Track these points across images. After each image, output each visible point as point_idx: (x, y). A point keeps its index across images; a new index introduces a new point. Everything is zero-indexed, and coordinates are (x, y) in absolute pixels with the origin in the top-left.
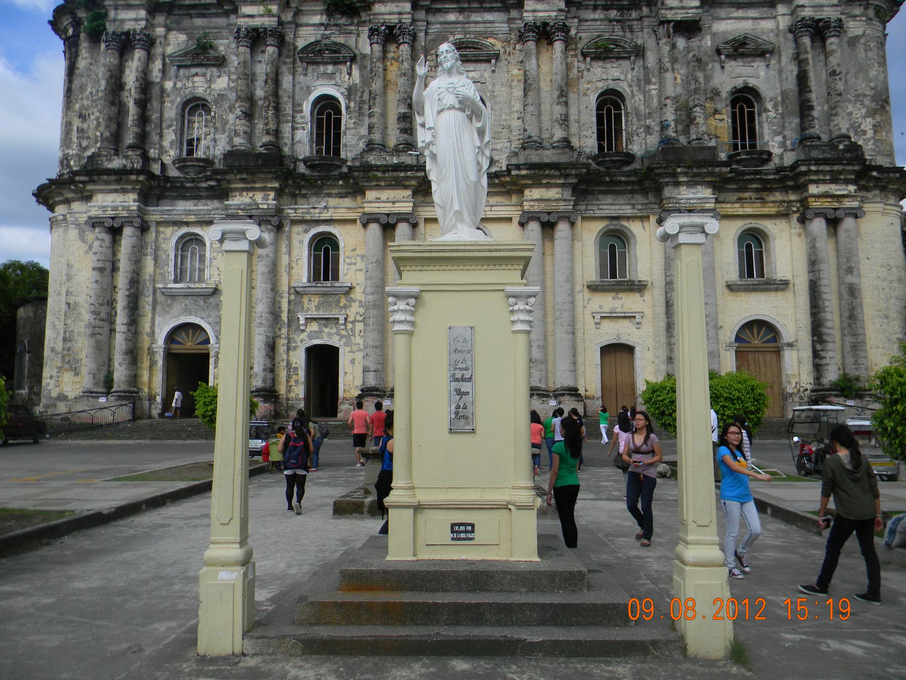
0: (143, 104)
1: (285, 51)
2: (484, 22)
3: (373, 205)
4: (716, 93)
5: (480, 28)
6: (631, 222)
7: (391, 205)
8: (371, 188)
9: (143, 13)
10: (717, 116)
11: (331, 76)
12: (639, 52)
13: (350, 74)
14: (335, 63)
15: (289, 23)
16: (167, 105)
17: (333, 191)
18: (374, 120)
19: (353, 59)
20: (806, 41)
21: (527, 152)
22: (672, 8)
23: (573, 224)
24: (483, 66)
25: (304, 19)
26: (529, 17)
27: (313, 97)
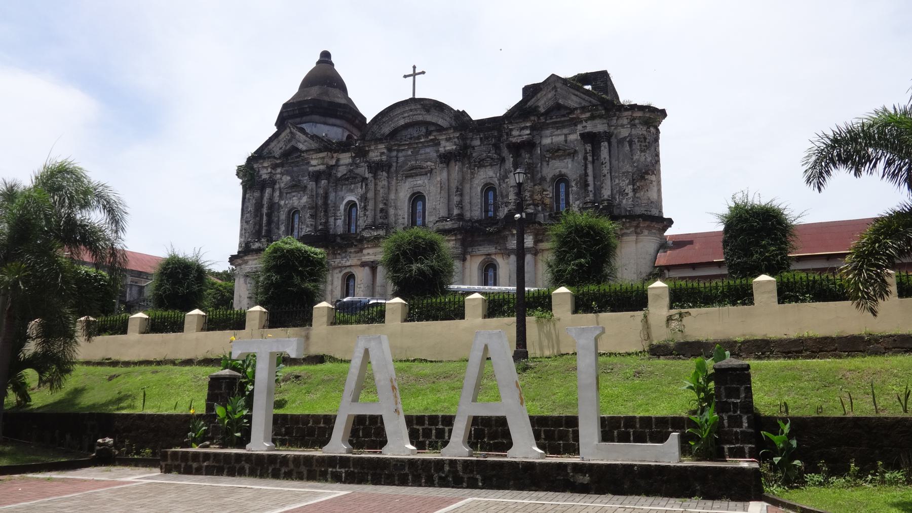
0: (269, 215)
1: (332, 180)
2: (425, 154)
3: (367, 257)
4: (543, 179)
5: (423, 157)
6: (497, 256)
7: (373, 257)
8: (365, 248)
9: (269, 170)
10: (544, 193)
11: (352, 191)
12: (503, 160)
13: (362, 188)
14: (354, 184)
15: (334, 166)
16: (282, 212)
17: (353, 250)
18: (367, 213)
19: (362, 182)
20: (589, 147)
21: (437, 224)
22: (514, 137)
23: (464, 260)
24: (423, 177)
25: (342, 162)
26: (442, 150)
27: (344, 202)
